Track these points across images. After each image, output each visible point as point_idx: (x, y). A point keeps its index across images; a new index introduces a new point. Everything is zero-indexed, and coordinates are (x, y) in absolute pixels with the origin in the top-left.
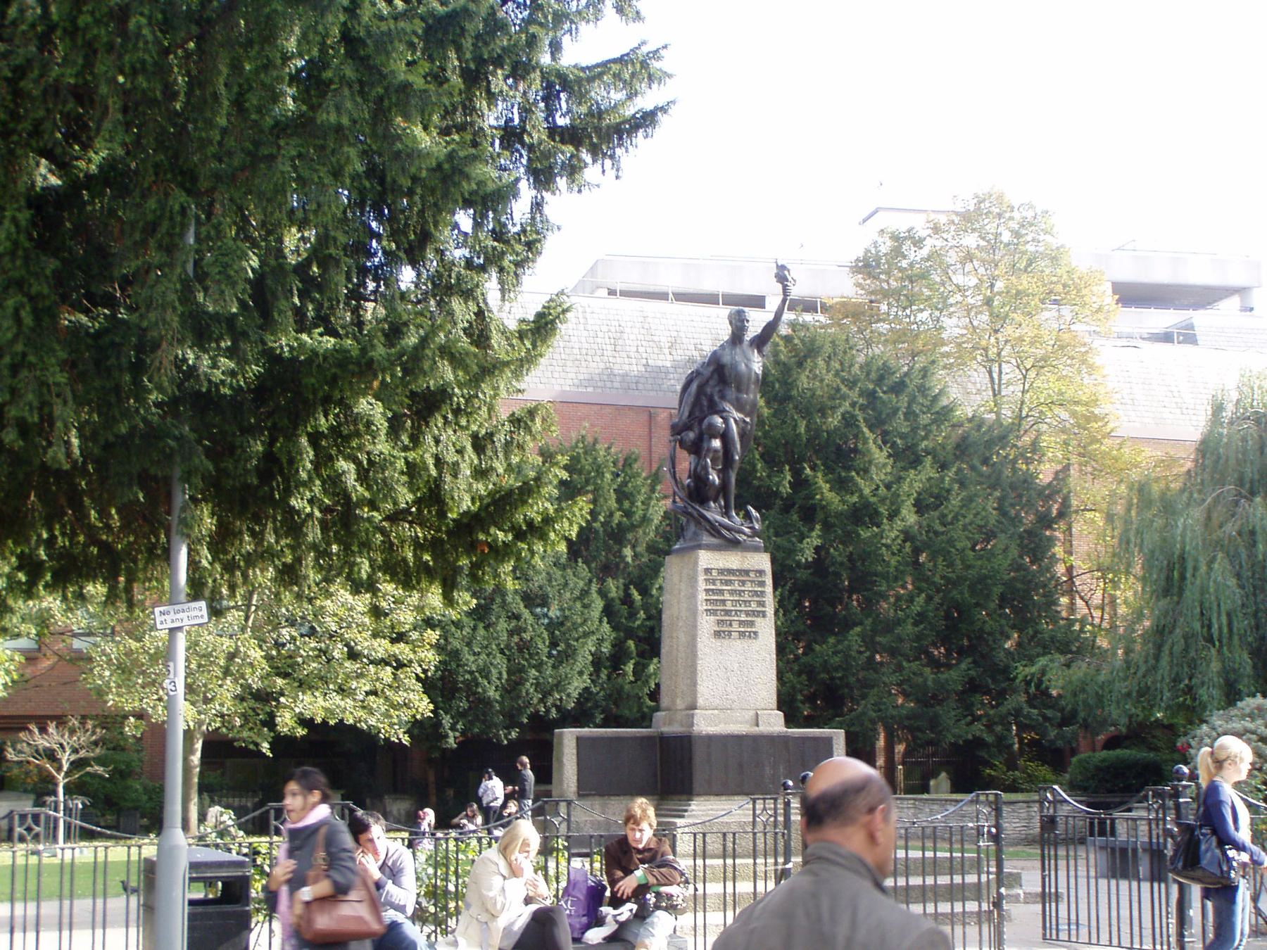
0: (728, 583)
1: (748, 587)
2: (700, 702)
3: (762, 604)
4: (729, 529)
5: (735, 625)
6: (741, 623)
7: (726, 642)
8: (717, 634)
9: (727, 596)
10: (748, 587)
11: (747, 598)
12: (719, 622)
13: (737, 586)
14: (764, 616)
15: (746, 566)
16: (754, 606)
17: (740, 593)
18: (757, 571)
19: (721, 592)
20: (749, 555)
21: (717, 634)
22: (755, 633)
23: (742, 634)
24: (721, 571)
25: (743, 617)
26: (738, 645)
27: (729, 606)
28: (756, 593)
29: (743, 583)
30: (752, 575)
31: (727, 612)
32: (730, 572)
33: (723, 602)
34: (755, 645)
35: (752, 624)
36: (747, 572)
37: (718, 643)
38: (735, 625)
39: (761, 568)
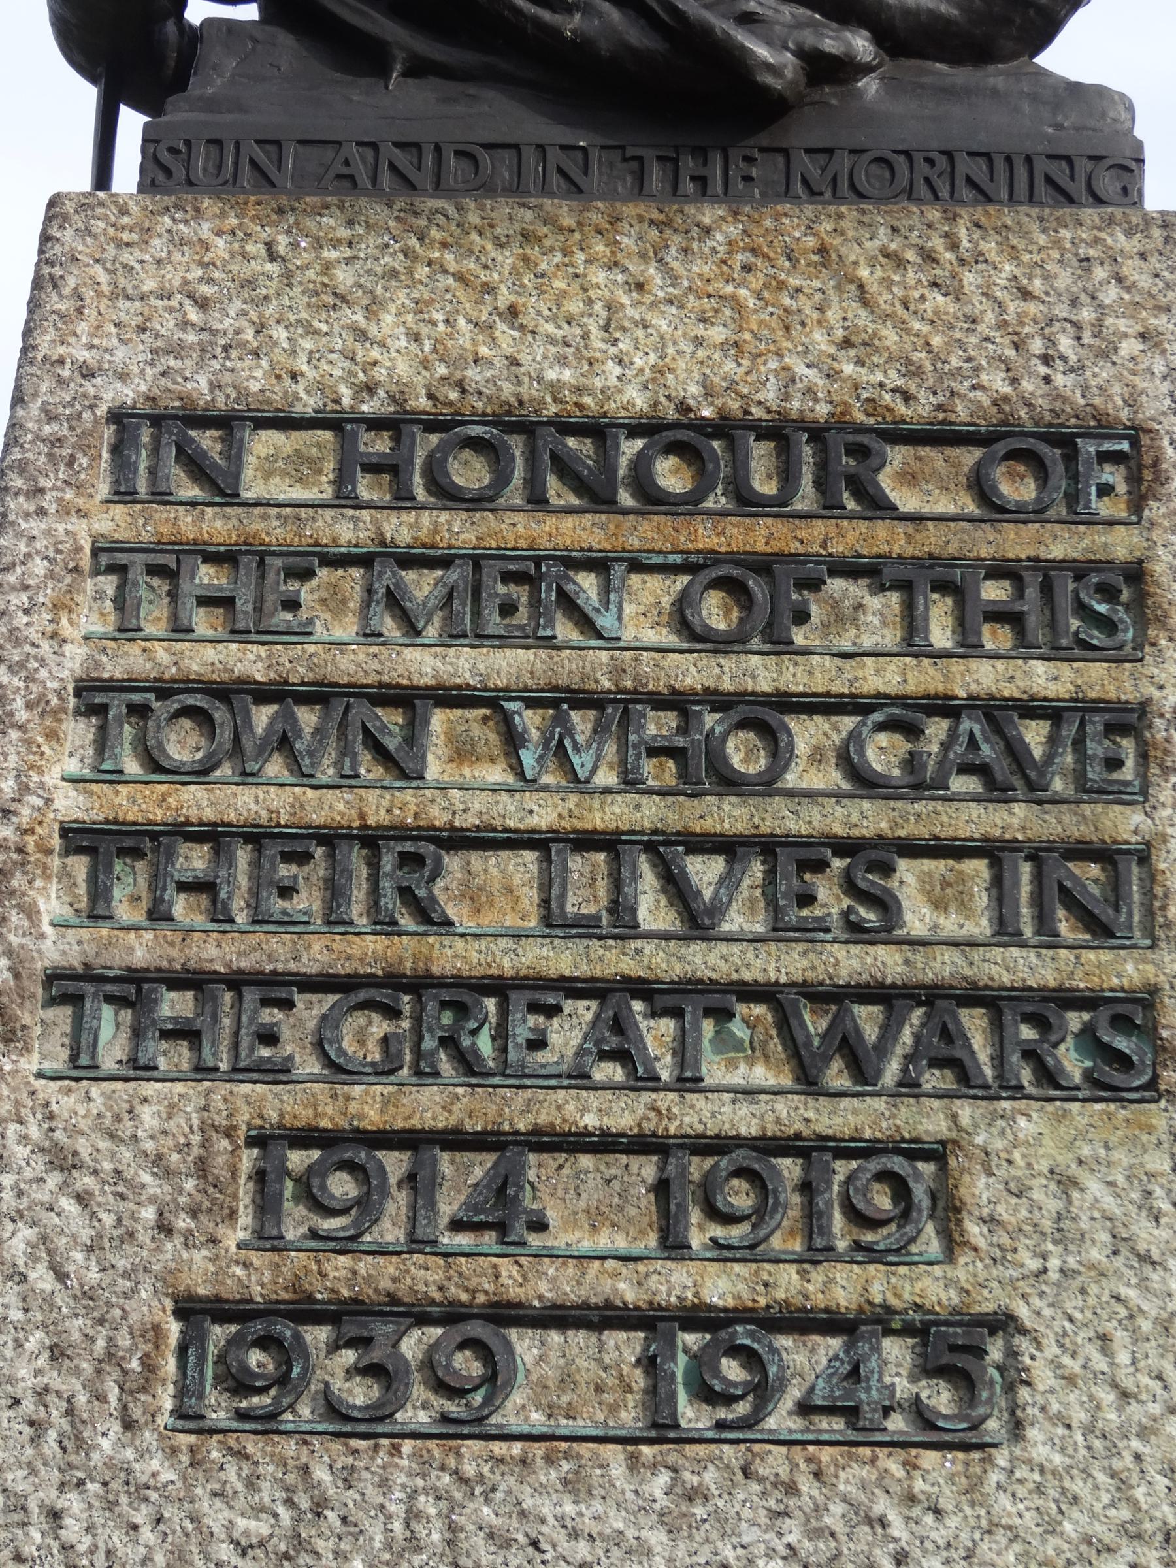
1: (858, 642)
6: (692, 1178)
7: (389, 1488)
9: (461, 781)
10: (858, 642)
11: (812, 790)
12: (303, 1166)
17: (692, 737)
18: (1004, 440)
19: (381, 721)
20: (863, 238)
22: (960, 1347)
23: (704, 1373)
24: (385, 444)
25: (741, 1090)
27: (491, 921)
28: (994, 744)
29: (767, 595)
30: (924, 492)
31: (441, 1010)
32: (561, 447)
35: (914, 1189)
36: (842, 455)
37: (243, 1498)
38: (590, 1233)
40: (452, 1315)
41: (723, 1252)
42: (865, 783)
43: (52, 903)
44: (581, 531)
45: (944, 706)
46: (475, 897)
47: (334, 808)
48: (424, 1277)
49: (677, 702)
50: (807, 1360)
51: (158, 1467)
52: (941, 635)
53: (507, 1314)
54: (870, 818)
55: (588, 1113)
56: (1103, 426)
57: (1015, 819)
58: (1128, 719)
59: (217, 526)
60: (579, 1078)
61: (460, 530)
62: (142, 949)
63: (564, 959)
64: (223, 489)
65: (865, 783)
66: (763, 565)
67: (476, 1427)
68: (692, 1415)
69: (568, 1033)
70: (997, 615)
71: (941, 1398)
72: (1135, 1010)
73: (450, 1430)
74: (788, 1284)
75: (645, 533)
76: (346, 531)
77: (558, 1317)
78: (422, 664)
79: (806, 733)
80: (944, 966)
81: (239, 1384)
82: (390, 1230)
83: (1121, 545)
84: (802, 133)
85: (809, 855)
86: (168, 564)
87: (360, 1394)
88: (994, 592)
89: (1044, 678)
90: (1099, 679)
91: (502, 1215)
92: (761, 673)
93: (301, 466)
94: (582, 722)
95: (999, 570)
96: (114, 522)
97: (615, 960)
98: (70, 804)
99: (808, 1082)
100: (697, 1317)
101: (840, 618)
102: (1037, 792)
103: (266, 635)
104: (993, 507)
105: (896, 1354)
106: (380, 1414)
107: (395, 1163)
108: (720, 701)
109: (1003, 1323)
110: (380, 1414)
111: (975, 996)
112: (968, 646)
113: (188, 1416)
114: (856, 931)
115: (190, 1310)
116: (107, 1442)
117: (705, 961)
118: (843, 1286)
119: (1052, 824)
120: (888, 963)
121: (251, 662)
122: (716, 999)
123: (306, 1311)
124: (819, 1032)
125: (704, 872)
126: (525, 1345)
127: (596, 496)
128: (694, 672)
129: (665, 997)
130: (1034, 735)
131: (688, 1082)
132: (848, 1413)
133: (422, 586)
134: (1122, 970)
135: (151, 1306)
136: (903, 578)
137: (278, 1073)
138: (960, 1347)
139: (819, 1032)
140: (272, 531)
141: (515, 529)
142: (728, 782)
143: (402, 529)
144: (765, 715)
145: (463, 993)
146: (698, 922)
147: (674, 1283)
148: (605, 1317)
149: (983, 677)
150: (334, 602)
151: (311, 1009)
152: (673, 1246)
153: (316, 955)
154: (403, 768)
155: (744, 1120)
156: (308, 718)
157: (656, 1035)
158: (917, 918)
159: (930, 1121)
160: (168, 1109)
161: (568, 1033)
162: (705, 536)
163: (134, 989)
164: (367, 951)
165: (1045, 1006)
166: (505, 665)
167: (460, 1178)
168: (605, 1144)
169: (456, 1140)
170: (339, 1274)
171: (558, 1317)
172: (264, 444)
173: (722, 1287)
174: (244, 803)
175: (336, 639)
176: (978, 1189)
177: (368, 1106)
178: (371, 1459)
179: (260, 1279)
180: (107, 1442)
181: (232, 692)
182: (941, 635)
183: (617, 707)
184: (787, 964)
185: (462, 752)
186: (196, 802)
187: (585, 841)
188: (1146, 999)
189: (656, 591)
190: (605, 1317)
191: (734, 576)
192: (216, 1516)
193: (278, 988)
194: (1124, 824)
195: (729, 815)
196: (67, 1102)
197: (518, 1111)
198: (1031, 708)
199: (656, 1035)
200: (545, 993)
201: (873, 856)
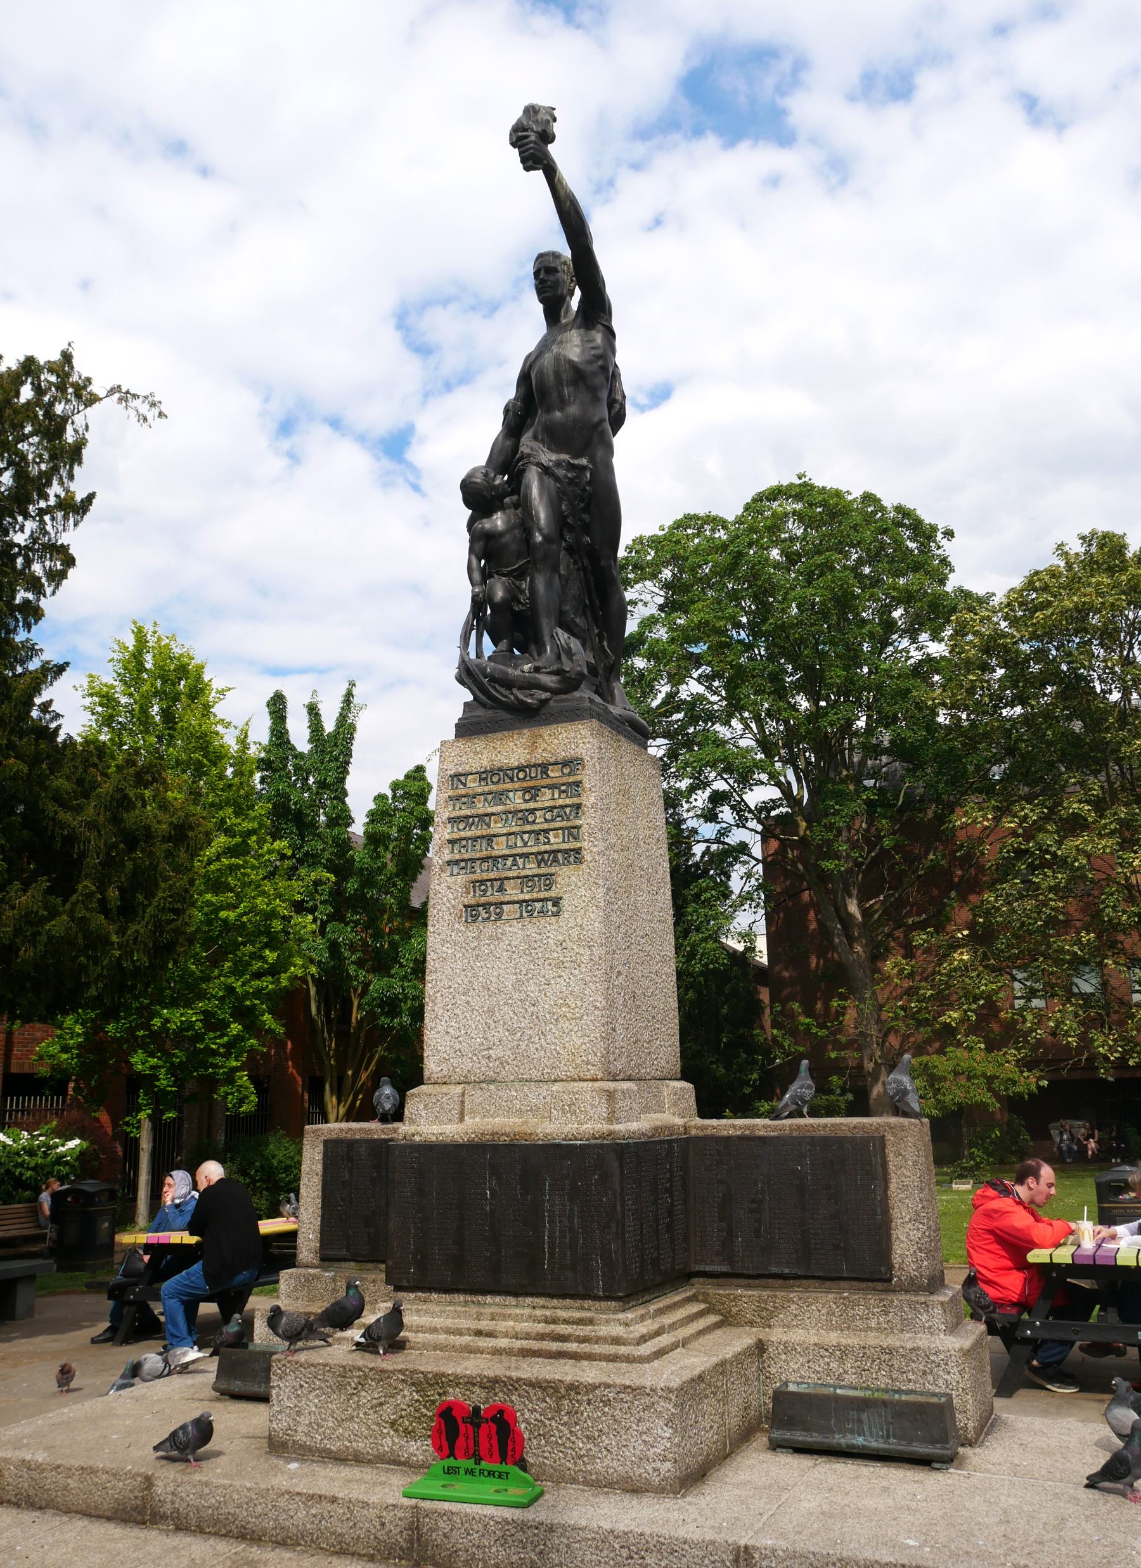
0: (500, 796)
2: (432, 1066)
3: (573, 832)
4: (508, 684)
5: (513, 892)
7: (489, 928)
8: (472, 912)
9: (497, 827)
10: (546, 798)
13: (517, 801)
14: (579, 861)
15: (539, 756)
16: (556, 841)
17: (525, 815)
18: (565, 763)
21: (472, 912)
24: (485, 775)
25: (531, 868)
26: (515, 930)
27: (500, 847)
29: (533, 792)
33: (490, 838)
34: (552, 930)
35: (548, 880)
36: (544, 767)
38: (513, 892)
39: (571, 753)
40: (496, 904)
41: (528, 892)
42: (546, 820)
43: (447, 851)
44: (509, 786)
45: (555, 807)
46: (497, 844)
47: (479, 833)
48: (492, 899)
49: (521, 811)
50: (538, 905)
51: (462, 928)
52: (556, 796)
53: (502, 903)
54: (546, 826)
55: (511, 874)
56: (577, 759)
57: (564, 824)
58: (578, 806)
59: (463, 792)
60: (510, 869)
61: (494, 788)
62: (457, 857)
63: (507, 852)
64: (465, 785)
65: (546, 820)
66: (532, 788)
67: (500, 919)
68: (525, 915)
69: (509, 862)
70: (564, 792)
71: (555, 909)
72: (578, 851)
73: (496, 920)
74: (535, 895)
75: (517, 785)
76: (480, 790)
77: (508, 903)
78: (490, 810)
79: (538, 813)
80: (555, 847)
81: (472, 916)
82: (489, 893)
83: (579, 778)
84: (543, 711)
85: (538, 833)
86: (458, 798)
87: (486, 916)
88: (563, 788)
89: (568, 801)
90: (575, 800)
91: (501, 889)
92: (532, 805)
93: (474, 780)
94: (510, 816)
95: (563, 784)
96: (451, 793)
97: (514, 851)
98: (448, 837)
99: (539, 866)
100: (525, 901)
101: (544, 794)
102: (568, 819)
103: (471, 808)
104: (564, 775)
105: (550, 903)
106: (489, 918)
107: (489, 884)
108: (527, 810)
109: (561, 898)
110: (489, 918)
111: (559, 851)
112: (560, 797)
113: (466, 921)
114: (545, 844)
115: (465, 906)
116: (457, 926)
117: (525, 850)
118: (542, 895)
119: (570, 824)
120: (547, 847)
121: (468, 812)
122: (525, 856)
123: (479, 905)
124: (541, 858)
125: (526, 836)
126: (504, 907)
127: (512, 780)
128: (524, 806)
129: (521, 856)
130: (568, 810)
131: (524, 868)
132: (543, 913)
133: (490, 797)
134: (579, 845)
135: (461, 907)
136: (552, 787)
137: (474, 872)
138: (556, 902)
139: (541, 858)
140: (471, 792)
141: (500, 787)
142: (529, 823)
143: (486, 789)
144: (532, 811)
145: (495, 858)
146: (525, 844)
147: (522, 897)
148: (514, 902)
149: (560, 802)
150: (479, 801)
151: (478, 862)
152: (522, 892)
153: (478, 856)
154: (489, 825)
155: (529, 873)
156: (476, 820)
157: (520, 861)
158: (552, 840)
159: (553, 870)
160: (461, 879)
161: (509, 862)
162: (525, 785)
163: (457, 862)
164: (484, 854)
165: (566, 852)
166: (500, 808)
167: (497, 884)
168: (513, 878)
169: (495, 880)
170: (483, 900)
171: (508, 903)
172: (470, 777)
173: (527, 897)
174: (468, 833)
175: (481, 807)
176: (559, 879)
177: (485, 876)
178: (486, 924)
179: (473, 902)
180: (457, 926)
181: (467, 817)
182: (556, 796)
183: (514, 813)
184: (535, 849)
185: (496, 822)
186: (463, 834)
187: (510, 834)
188: (580, 849)
189: (520, 794)
190: (514, 902)
191: (526, 790)
192: (469, 934)
193: (473, 860)
194: (578, 822)
195: (528, 828)
196: (449, 879)
197: (503, 875)
198: (567, 806)
199: (520, 861)
200: (505, 857)
201: (546, 831)
